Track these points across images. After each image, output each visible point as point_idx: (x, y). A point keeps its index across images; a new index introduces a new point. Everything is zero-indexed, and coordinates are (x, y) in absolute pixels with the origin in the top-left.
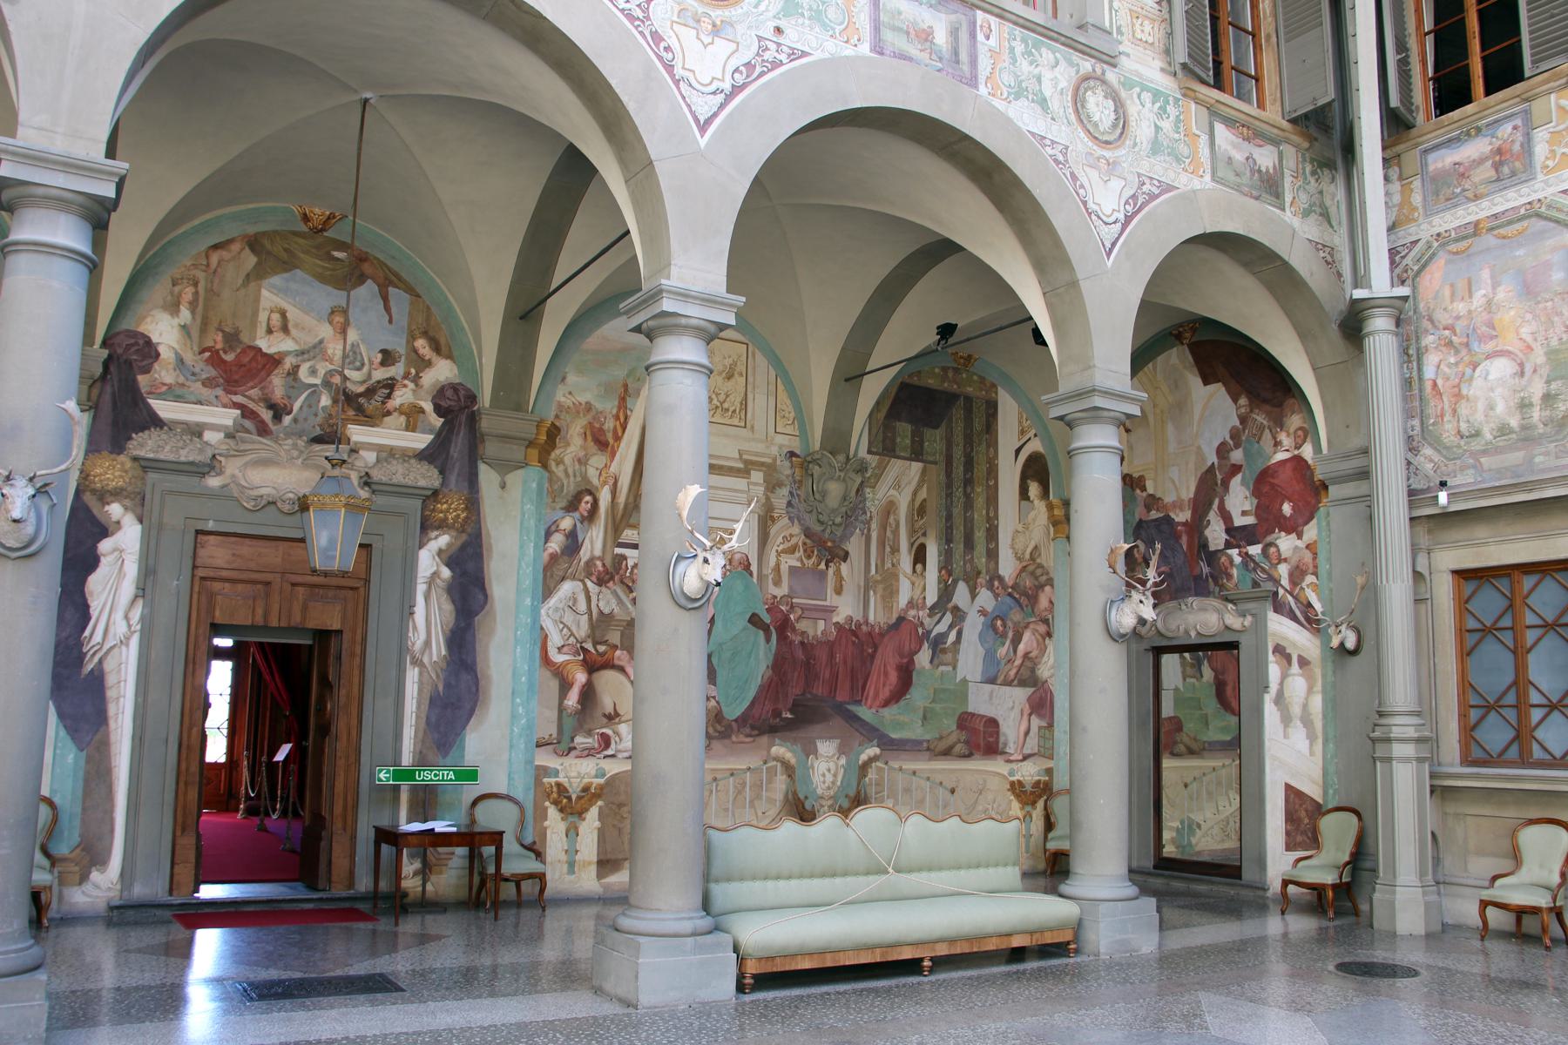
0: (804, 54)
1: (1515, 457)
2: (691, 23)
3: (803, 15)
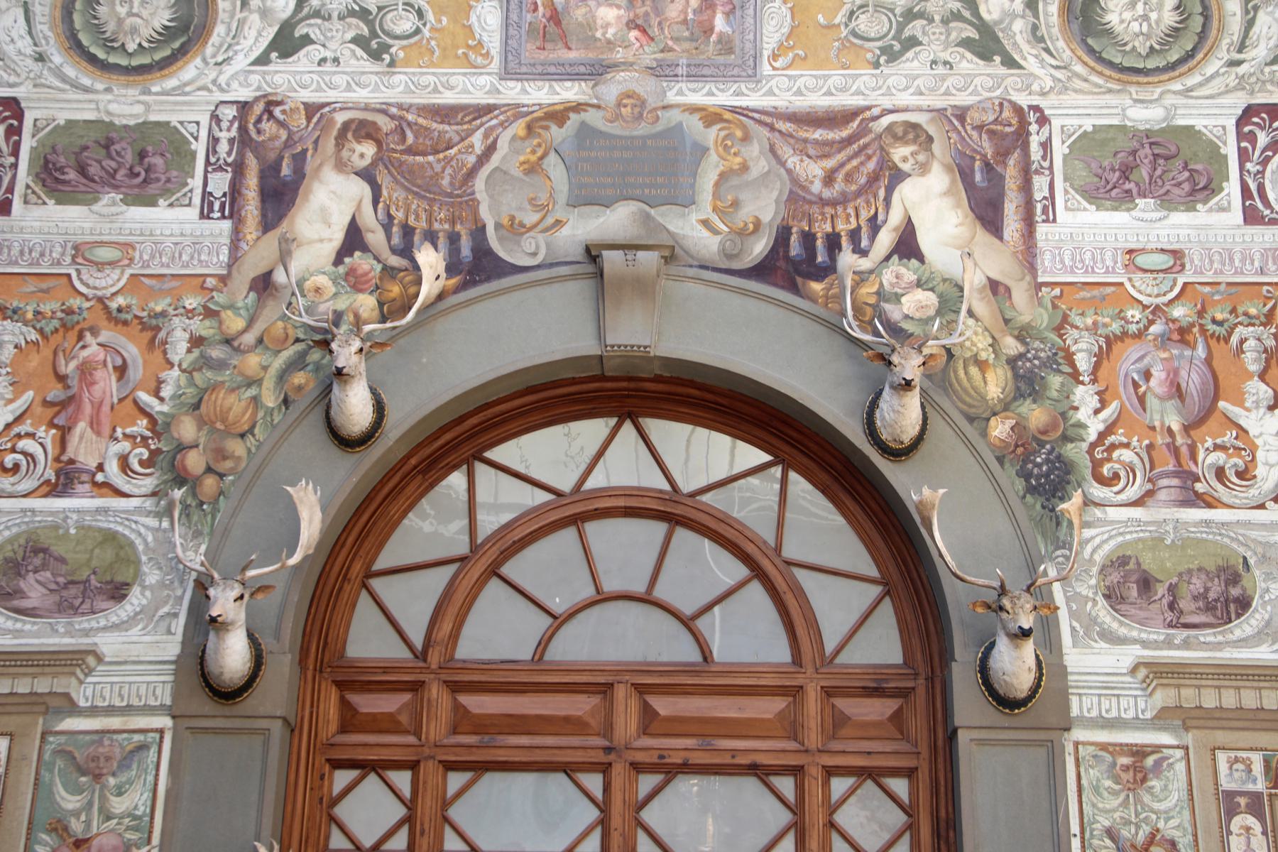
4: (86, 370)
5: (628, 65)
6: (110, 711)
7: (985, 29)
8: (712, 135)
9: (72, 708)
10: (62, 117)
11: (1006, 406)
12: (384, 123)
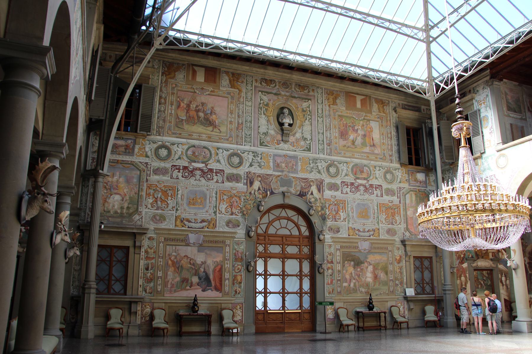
1: (119, 220)
4: (233, 202)
5: (285, 171)
6: (239, 238)
7: (319, 170)
8: (294, 180)
9: (235, 238)
10: (228, 172)
11: (320, 211)
12: (262, 176)
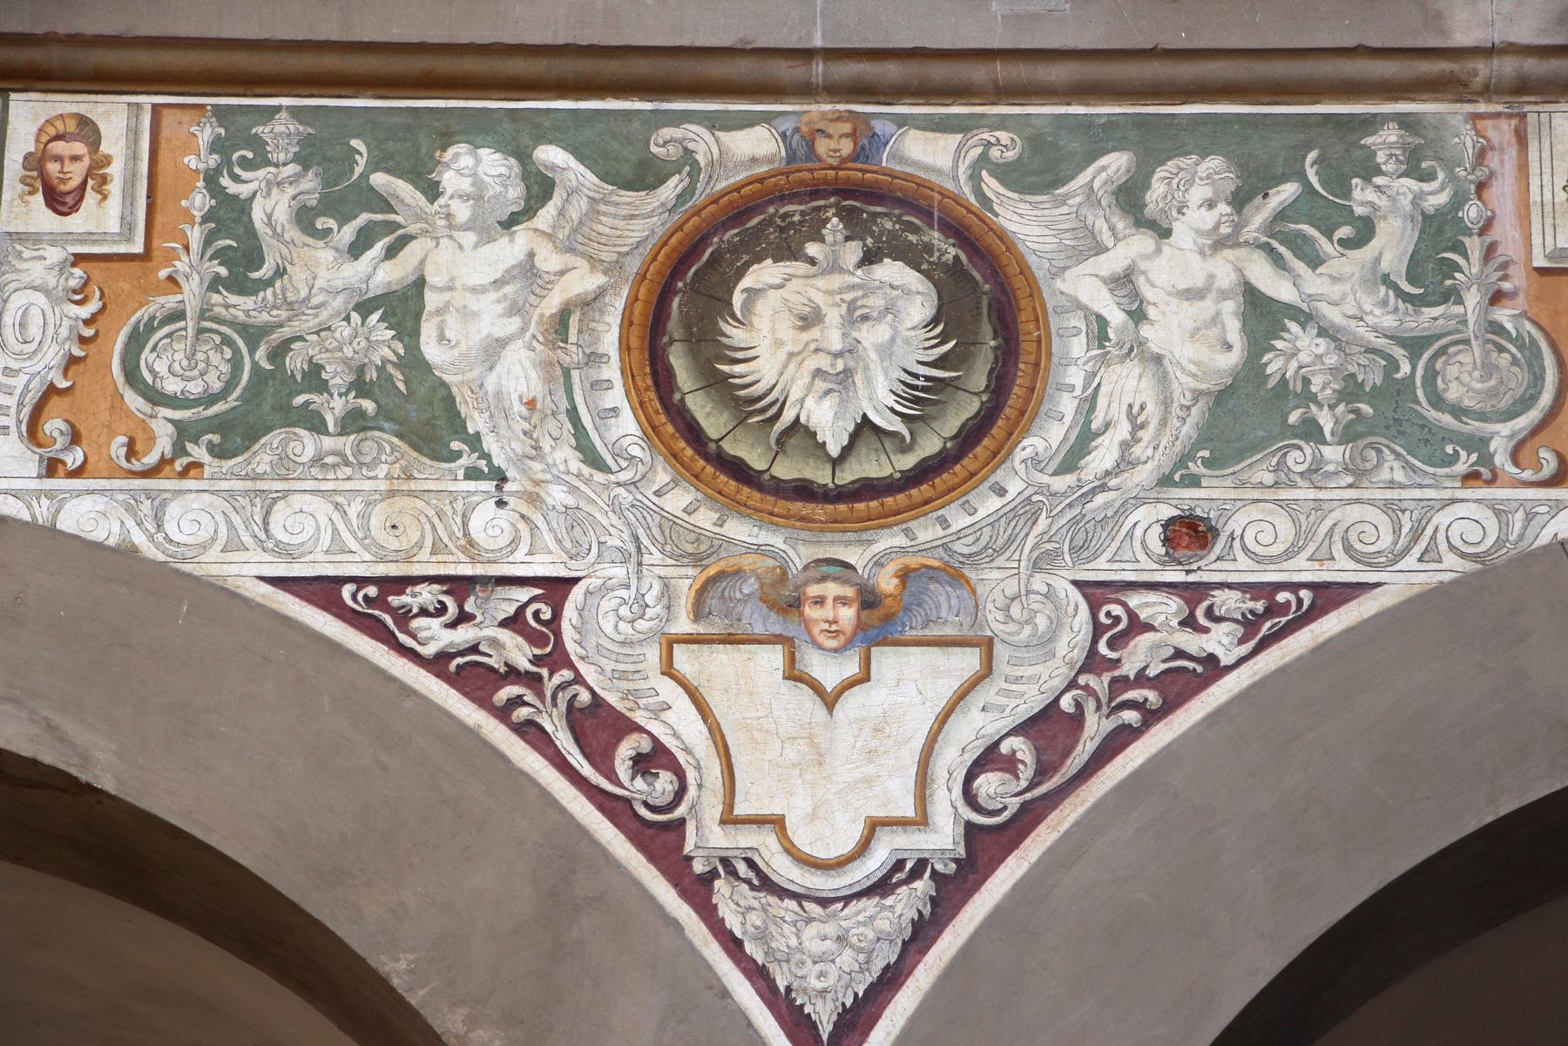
0: (1329, 596)
2: (758, 620)
3: (1311, 431)
